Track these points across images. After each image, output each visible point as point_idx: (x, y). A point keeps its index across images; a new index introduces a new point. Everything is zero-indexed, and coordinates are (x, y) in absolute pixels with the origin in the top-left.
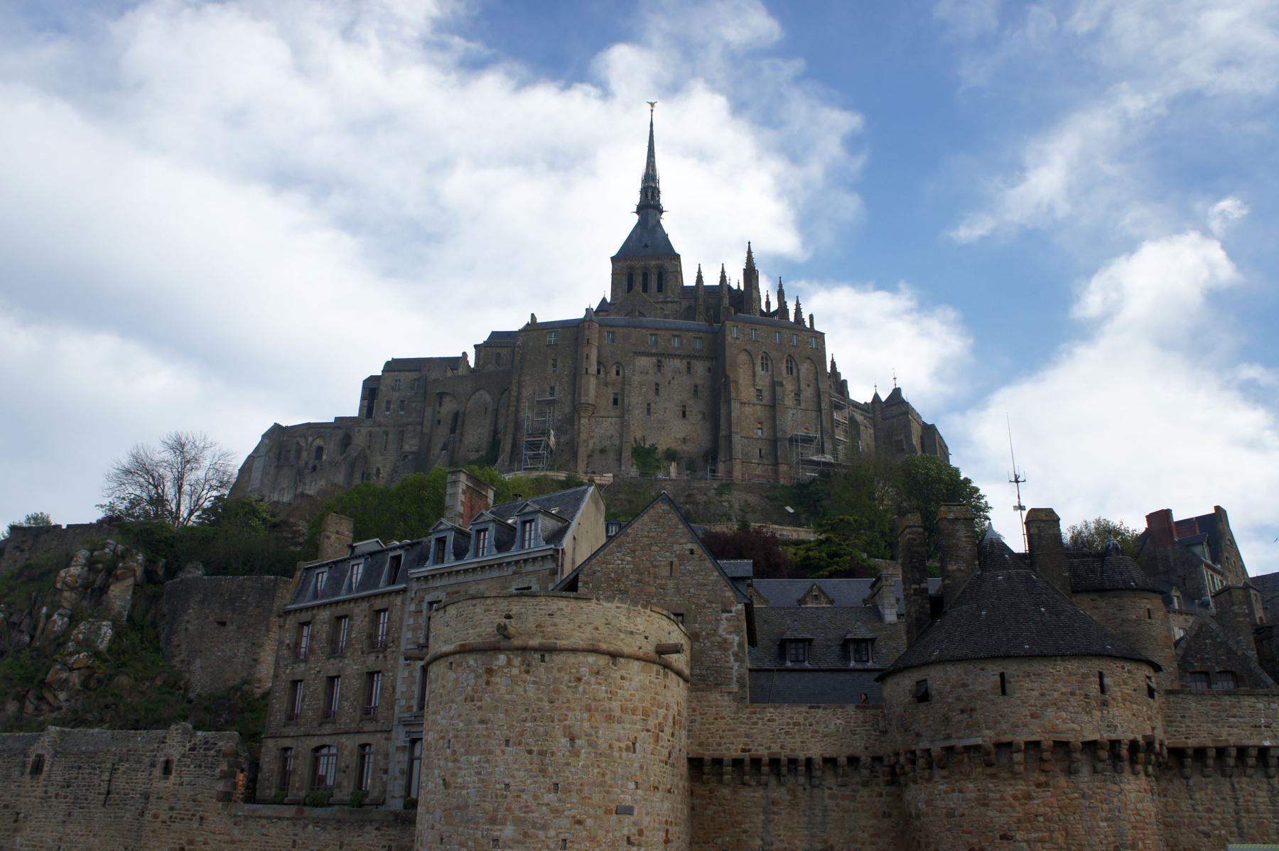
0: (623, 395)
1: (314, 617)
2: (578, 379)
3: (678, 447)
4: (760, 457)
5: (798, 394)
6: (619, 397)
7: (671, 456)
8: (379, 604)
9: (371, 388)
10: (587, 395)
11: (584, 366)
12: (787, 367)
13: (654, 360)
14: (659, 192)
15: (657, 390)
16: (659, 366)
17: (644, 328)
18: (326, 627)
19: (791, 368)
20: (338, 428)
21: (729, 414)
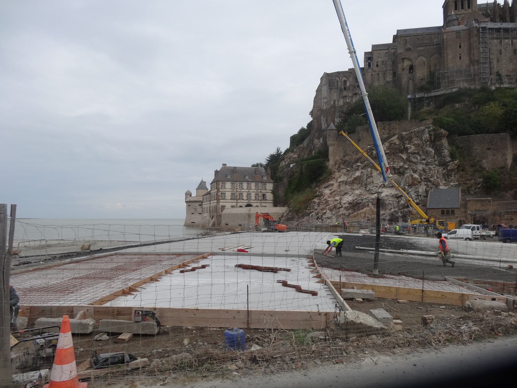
16: (501, 42)
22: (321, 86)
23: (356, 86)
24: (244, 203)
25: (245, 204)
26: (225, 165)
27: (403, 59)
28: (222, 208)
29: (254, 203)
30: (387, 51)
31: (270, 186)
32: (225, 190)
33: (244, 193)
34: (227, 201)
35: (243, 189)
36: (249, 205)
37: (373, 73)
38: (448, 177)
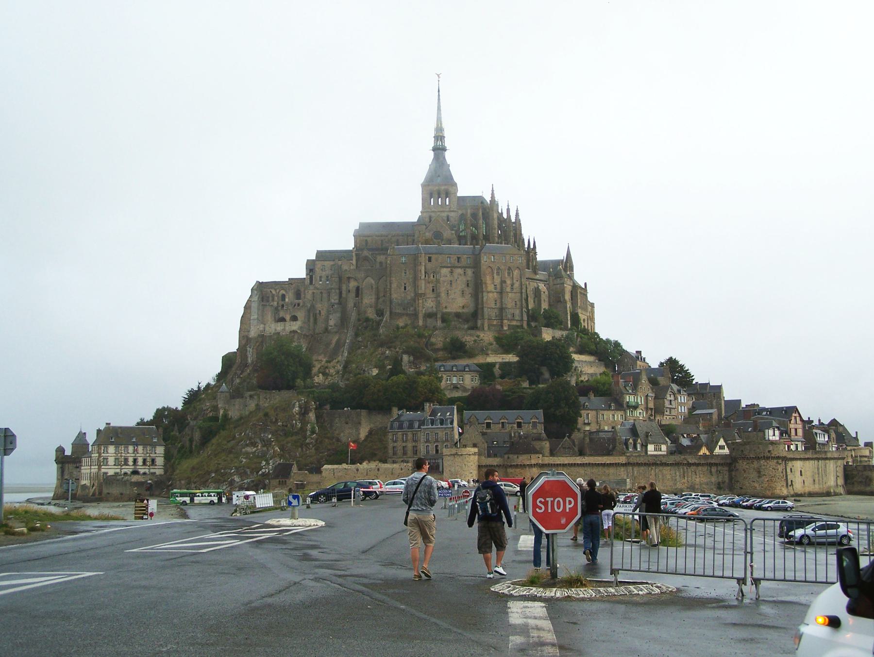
0: (436, 287)
1: (397, 434)
2: (417, 283)
3: (460, 311)
4: (496, 316)
5: (512, 285)
6: (435, 288)
7: (458, 315)
8: (414, 432)
9: (311, 267)
10: (421, 289)
11: (420, 276)
12: (508, 273)
13: (449, 269)
14: (444, 137)
15: (451, 284)
16: (452, 272)
17: (444, 254)
18: (401, 436)
19: (510, 273)
20: (291, 284)
21: (483, 297)
22: (251, 301)
23: (296, 305)
24: (128, 469)
25: (131, 470)
26: (109, 424)
27: (349, 278)
28: (103, 475)
29: (141, 469)
30: (332, 263)
31: (160, 450)
32: (107, 455)
33: (130, 458)
34: (109, 467)
35: (128, 453)
36: (135, 472)
37: (314, 291)
38: (306, 449)
